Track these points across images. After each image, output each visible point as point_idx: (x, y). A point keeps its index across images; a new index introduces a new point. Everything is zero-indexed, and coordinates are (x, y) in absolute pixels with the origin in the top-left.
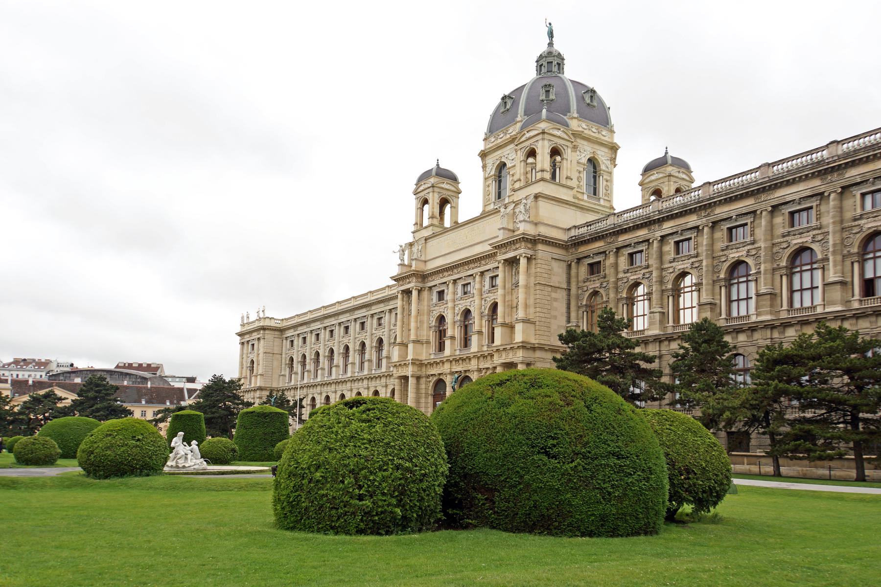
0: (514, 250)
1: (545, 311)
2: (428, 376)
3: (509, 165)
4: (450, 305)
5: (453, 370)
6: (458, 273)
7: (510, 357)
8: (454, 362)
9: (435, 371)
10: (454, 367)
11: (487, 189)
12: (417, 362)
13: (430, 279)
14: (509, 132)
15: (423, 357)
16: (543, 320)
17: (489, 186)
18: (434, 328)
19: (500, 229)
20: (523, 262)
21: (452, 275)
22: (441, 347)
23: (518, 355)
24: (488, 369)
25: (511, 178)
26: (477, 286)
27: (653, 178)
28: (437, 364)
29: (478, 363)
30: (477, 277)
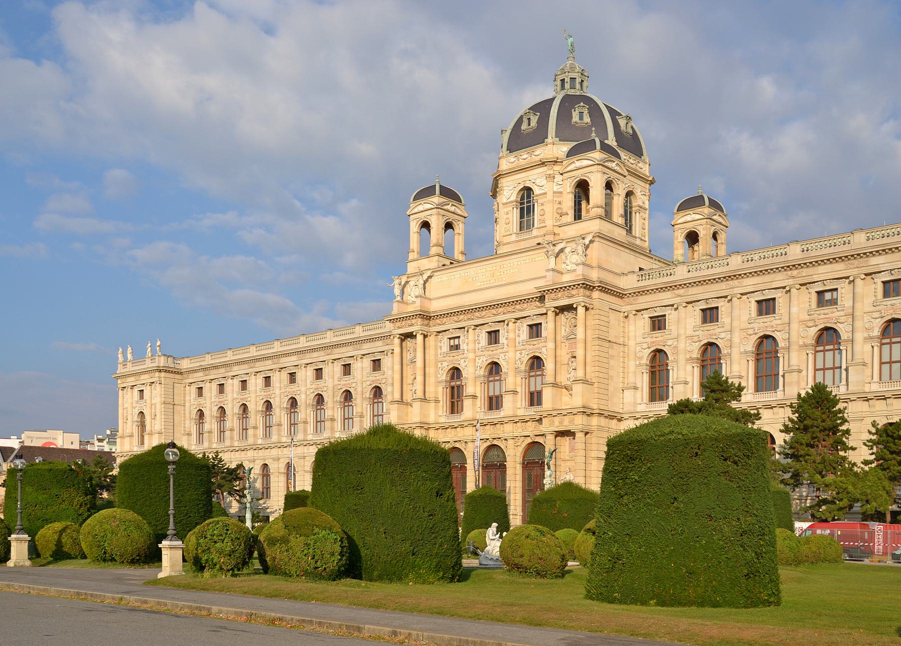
1: (603, 370)
3: (537, 191)
6: (482, 317)
11: (506, 216)
14: (537, 153)
15: (432, 419)
16: (602, 380)
17: (507, 213)
18: (444, 384)
19: (548, 271)
22: (455, 406)
25: (541, 208)
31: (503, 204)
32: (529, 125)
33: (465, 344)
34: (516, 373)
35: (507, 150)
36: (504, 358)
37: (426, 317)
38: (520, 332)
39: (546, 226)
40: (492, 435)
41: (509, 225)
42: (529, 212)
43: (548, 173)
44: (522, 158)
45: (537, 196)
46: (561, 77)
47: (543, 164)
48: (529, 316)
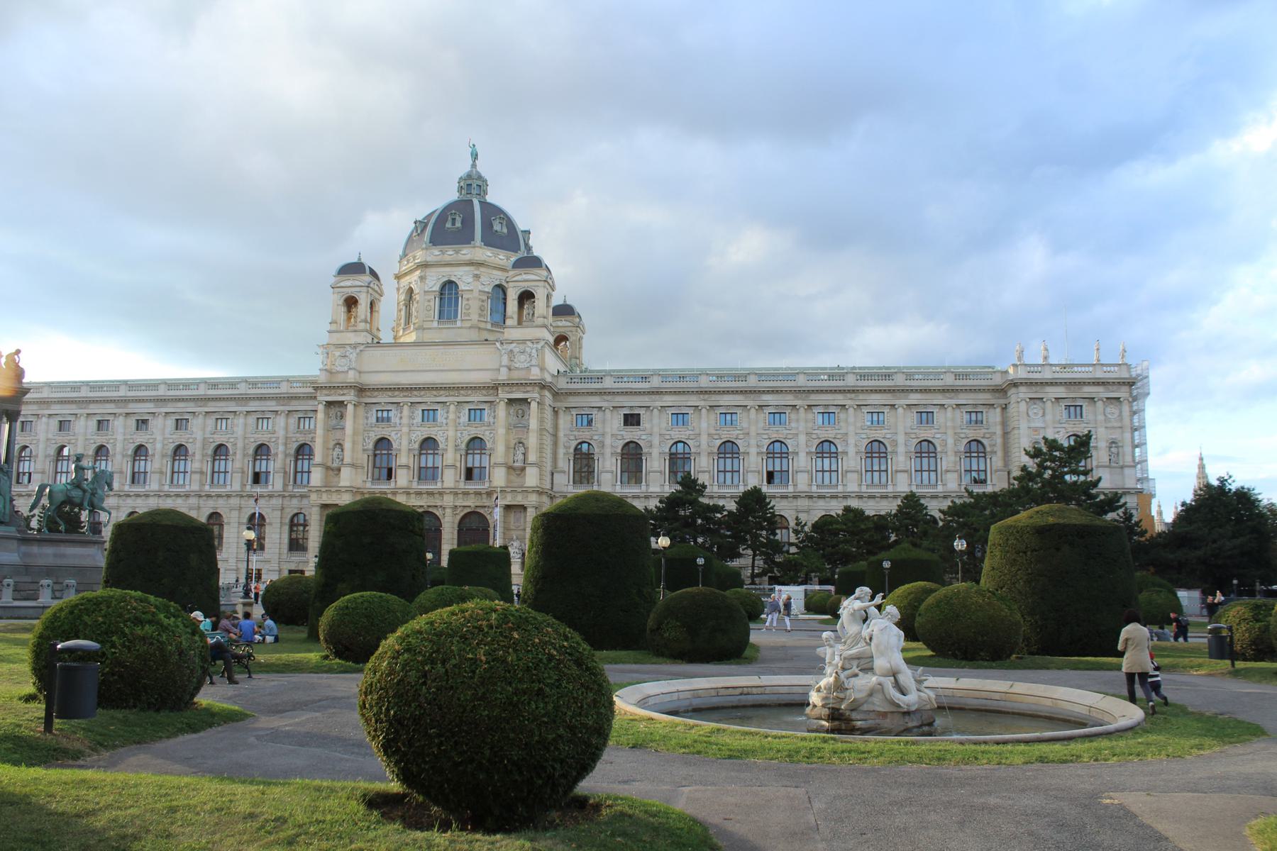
0: (524, 392)
3: (462, 287)
4: (405, 429)
6: (421, 396)
7: (519, 500)
8: (413, 496)
11: (426, 304)
12: (355, 490)
13: (368, 394)
14: (462, 252)
17: (429, 301)
20: (534, 405)
23: (529, 499)
26: (452, 416)
27: (560, 324)
30: (452, 406)
31: (425, 292)
32: (454, 224)
33: (398, 419)
37: (361, 390)
42: (450, 305)
45: (463, 291)
46: (469, 182)
47: (471, 263)
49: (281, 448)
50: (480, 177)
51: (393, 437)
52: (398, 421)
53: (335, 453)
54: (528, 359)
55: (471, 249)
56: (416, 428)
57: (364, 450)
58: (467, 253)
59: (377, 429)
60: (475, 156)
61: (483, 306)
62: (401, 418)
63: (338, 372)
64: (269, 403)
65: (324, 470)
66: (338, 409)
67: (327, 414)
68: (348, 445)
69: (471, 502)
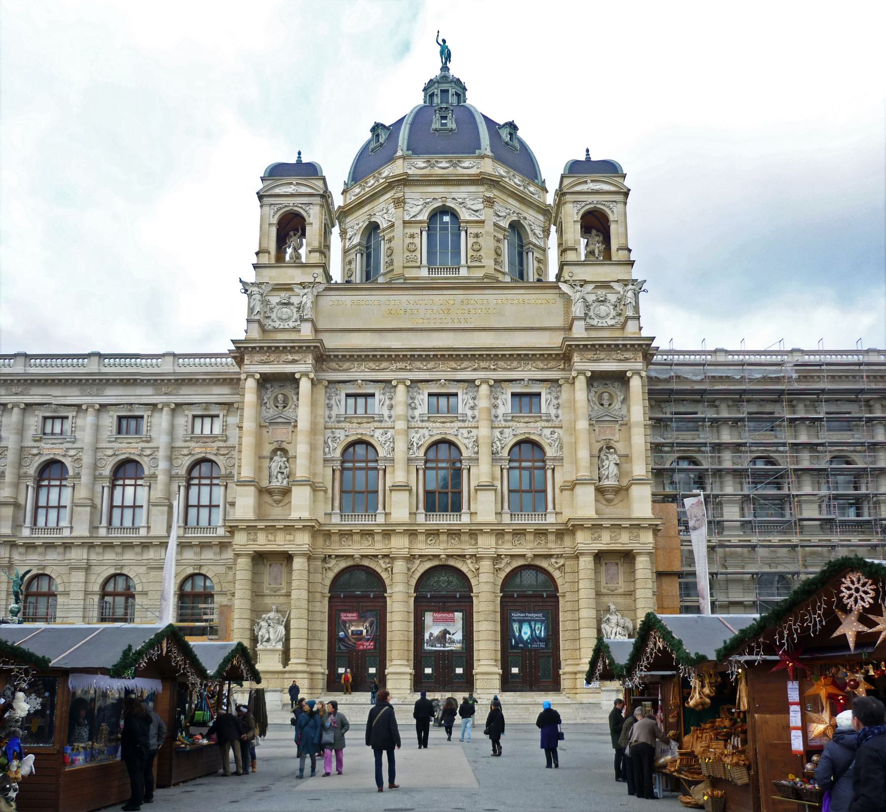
2: (326, 559)
3: (464, 215)
5: (416, 552)
7: (624, 541)
8: (422, 538)
9: (356, 548)
10: (420, 546)
11: (408, 241)
13: (334, 365)
14: (463, 165)
21: (410, 370)
24: (513, 556)
28: (368, 534)
29: (497, 543)
31: (405, 222)
34: (493, 460)
35: (408, 150)
36: (466, 435)
38: (499, 402)
39: (484, 267)
40: (449, 550)
41: (414, 254)
43: (488, 194)
44: (439, 165)
45: (467, 222)
46: (444, 86)
47: (481, 180)
48: (523, 380)
49: (163, 465)
50: (458, 82)
51: (377, 438)
52: (386, 412)
53: (273, 465)
54: (613, 313)
55: (478, 161)
56: (420, 424)
57: (325, 460)
58: (469, 167)
59: (348, 424)
60: (446, 54)
61: (500, 248)
62: (391, 407)
63: (276, 330)
64: (140, 391)
65: (257, 494)
66: (277, 391)
67: (261, 403)
68: (301, 449)
69: (528, 548)
